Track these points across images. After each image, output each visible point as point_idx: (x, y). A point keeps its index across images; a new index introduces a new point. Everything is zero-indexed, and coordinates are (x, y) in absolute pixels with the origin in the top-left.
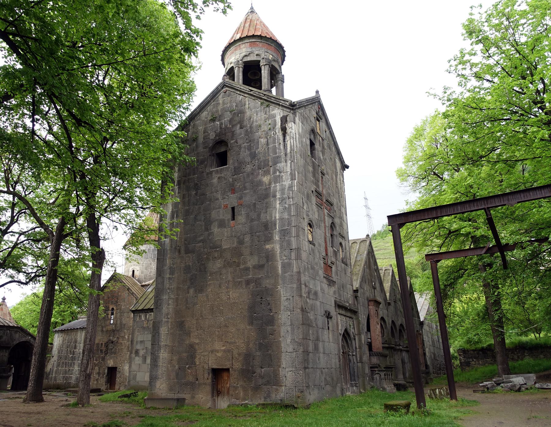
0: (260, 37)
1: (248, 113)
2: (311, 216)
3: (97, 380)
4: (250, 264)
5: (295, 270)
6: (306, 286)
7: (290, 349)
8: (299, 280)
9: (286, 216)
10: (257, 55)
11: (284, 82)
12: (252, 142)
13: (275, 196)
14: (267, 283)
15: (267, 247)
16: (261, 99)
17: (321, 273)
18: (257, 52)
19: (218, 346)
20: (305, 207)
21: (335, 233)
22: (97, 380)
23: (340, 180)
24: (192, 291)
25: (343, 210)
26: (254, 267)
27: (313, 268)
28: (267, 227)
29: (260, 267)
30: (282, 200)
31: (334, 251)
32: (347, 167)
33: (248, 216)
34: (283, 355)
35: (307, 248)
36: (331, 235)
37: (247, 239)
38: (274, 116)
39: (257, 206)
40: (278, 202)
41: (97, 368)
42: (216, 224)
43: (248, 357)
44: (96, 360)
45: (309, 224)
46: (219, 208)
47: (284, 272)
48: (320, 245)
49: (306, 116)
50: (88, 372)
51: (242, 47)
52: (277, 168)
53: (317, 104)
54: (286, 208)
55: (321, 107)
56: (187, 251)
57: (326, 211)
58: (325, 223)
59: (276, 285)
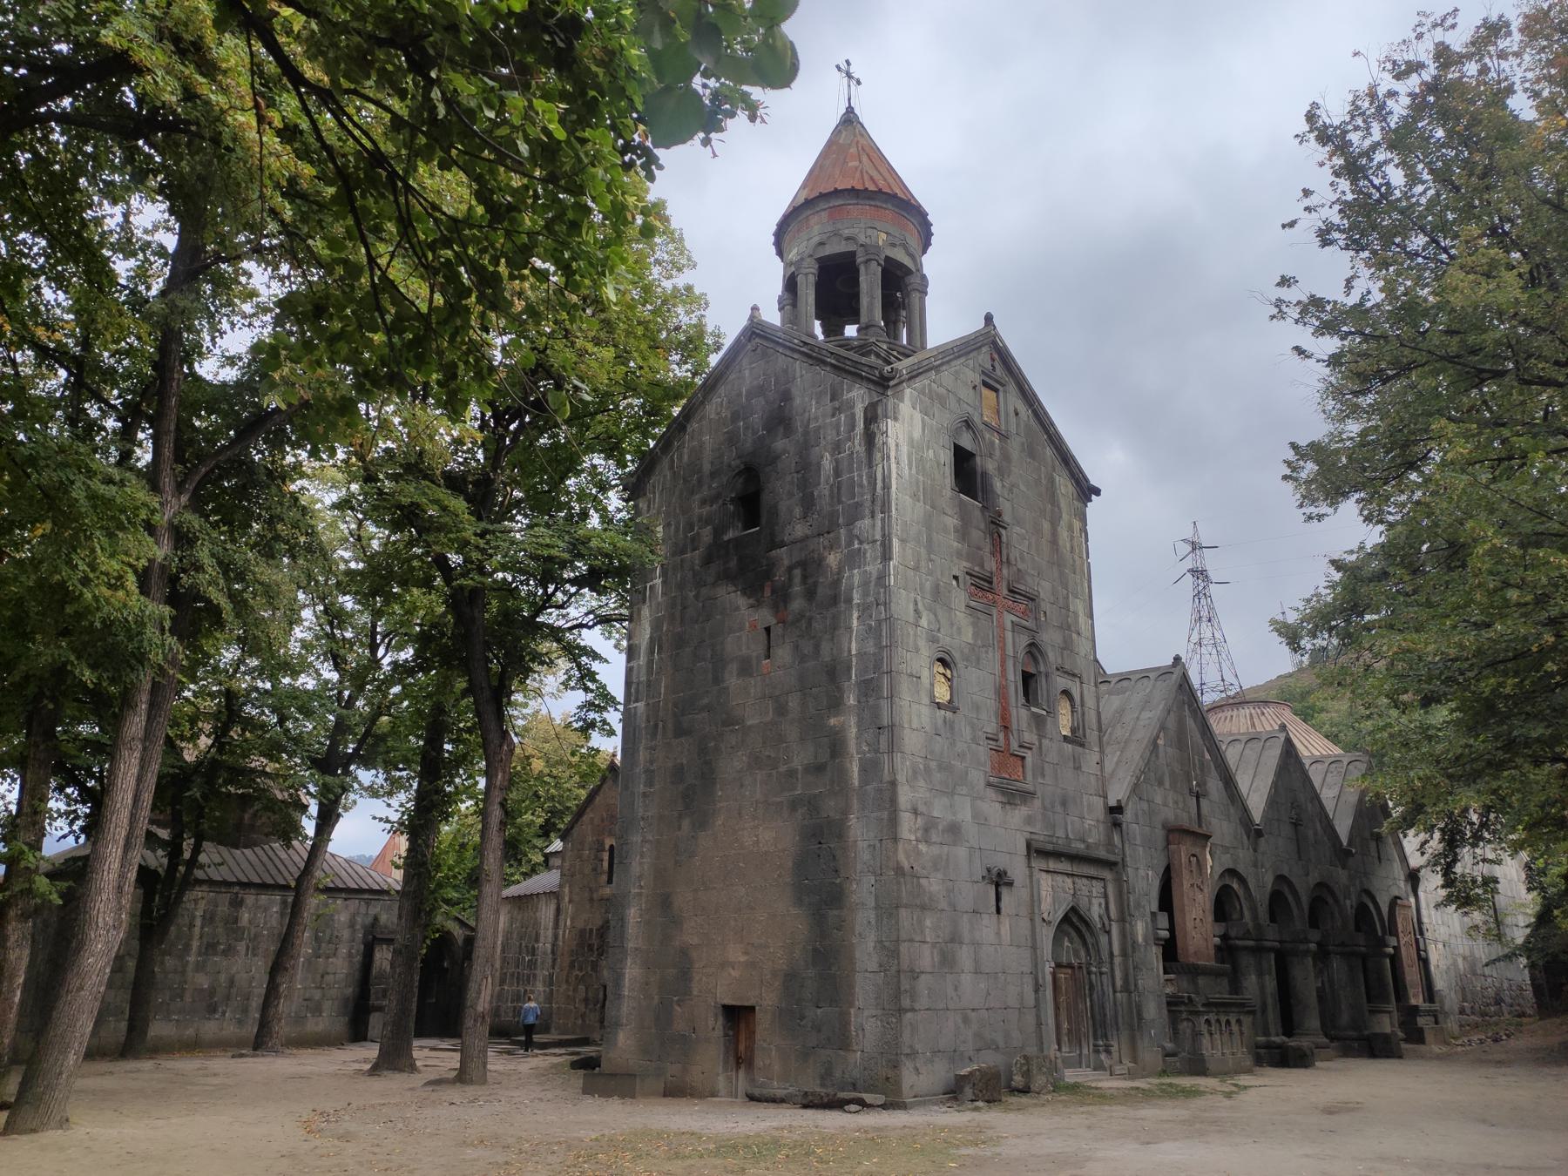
0: (853, 192)
1: (798, 401)
2: (945, 640)
3: (583, 1016)
4: (797, 763)
5: (886, 777)
6: (915, 812)
7: (873, 966)
8: (893, 801)
9: (871, 650)
10: (848, 239)
11: (926, 293)
12: (806, 469)
13: (849, 600)
14: (830, 808)
15: (832, 721)
16: (825, 363)
17: (977, 777)
18: (846, 232)
19: (736, 954)
20: (924, 622)
21: (1042, 669)
22: (583, 1016)
23: (1070, 528)
24: (686, 823)
25: (1078, 606)
26: (808, 769)
27: (945, 767)
28: (834, 673)
29: (819, 769)
30: (865, 609)
31: (1036, 717)
32: (1097, 492)
33: (796, 647)
34: (859, 978)
35: (926, 721)
36: (1027, 678)
37: (793, 703)
38: (850, 405)
39: (814, 624)
40: (855, 615)
41: (582, 987)
42: (733, 667)
43: (791, 979)
44: (580, 969)
45: (941, 660)
46: (741, 629)
47: (865, 781)
48: (977, 708)
49: (942, 391)
50: (480, 1009)
51: (814, 220)
52: (856, 531)
53: (984, 349)
54: (870, 627)
55: (1003, 356)
56: (680, 732)
57: (1009, 619)
58: (1003, 649)
59: (845, 812)
